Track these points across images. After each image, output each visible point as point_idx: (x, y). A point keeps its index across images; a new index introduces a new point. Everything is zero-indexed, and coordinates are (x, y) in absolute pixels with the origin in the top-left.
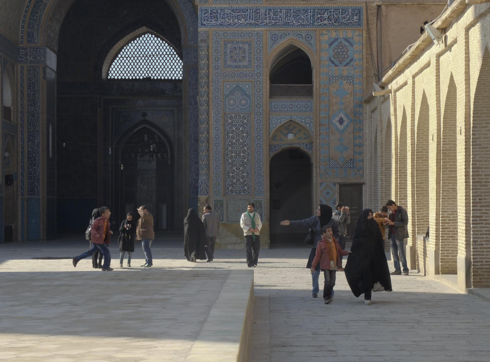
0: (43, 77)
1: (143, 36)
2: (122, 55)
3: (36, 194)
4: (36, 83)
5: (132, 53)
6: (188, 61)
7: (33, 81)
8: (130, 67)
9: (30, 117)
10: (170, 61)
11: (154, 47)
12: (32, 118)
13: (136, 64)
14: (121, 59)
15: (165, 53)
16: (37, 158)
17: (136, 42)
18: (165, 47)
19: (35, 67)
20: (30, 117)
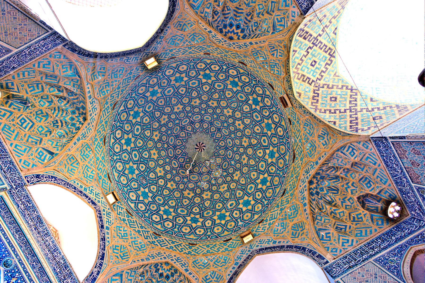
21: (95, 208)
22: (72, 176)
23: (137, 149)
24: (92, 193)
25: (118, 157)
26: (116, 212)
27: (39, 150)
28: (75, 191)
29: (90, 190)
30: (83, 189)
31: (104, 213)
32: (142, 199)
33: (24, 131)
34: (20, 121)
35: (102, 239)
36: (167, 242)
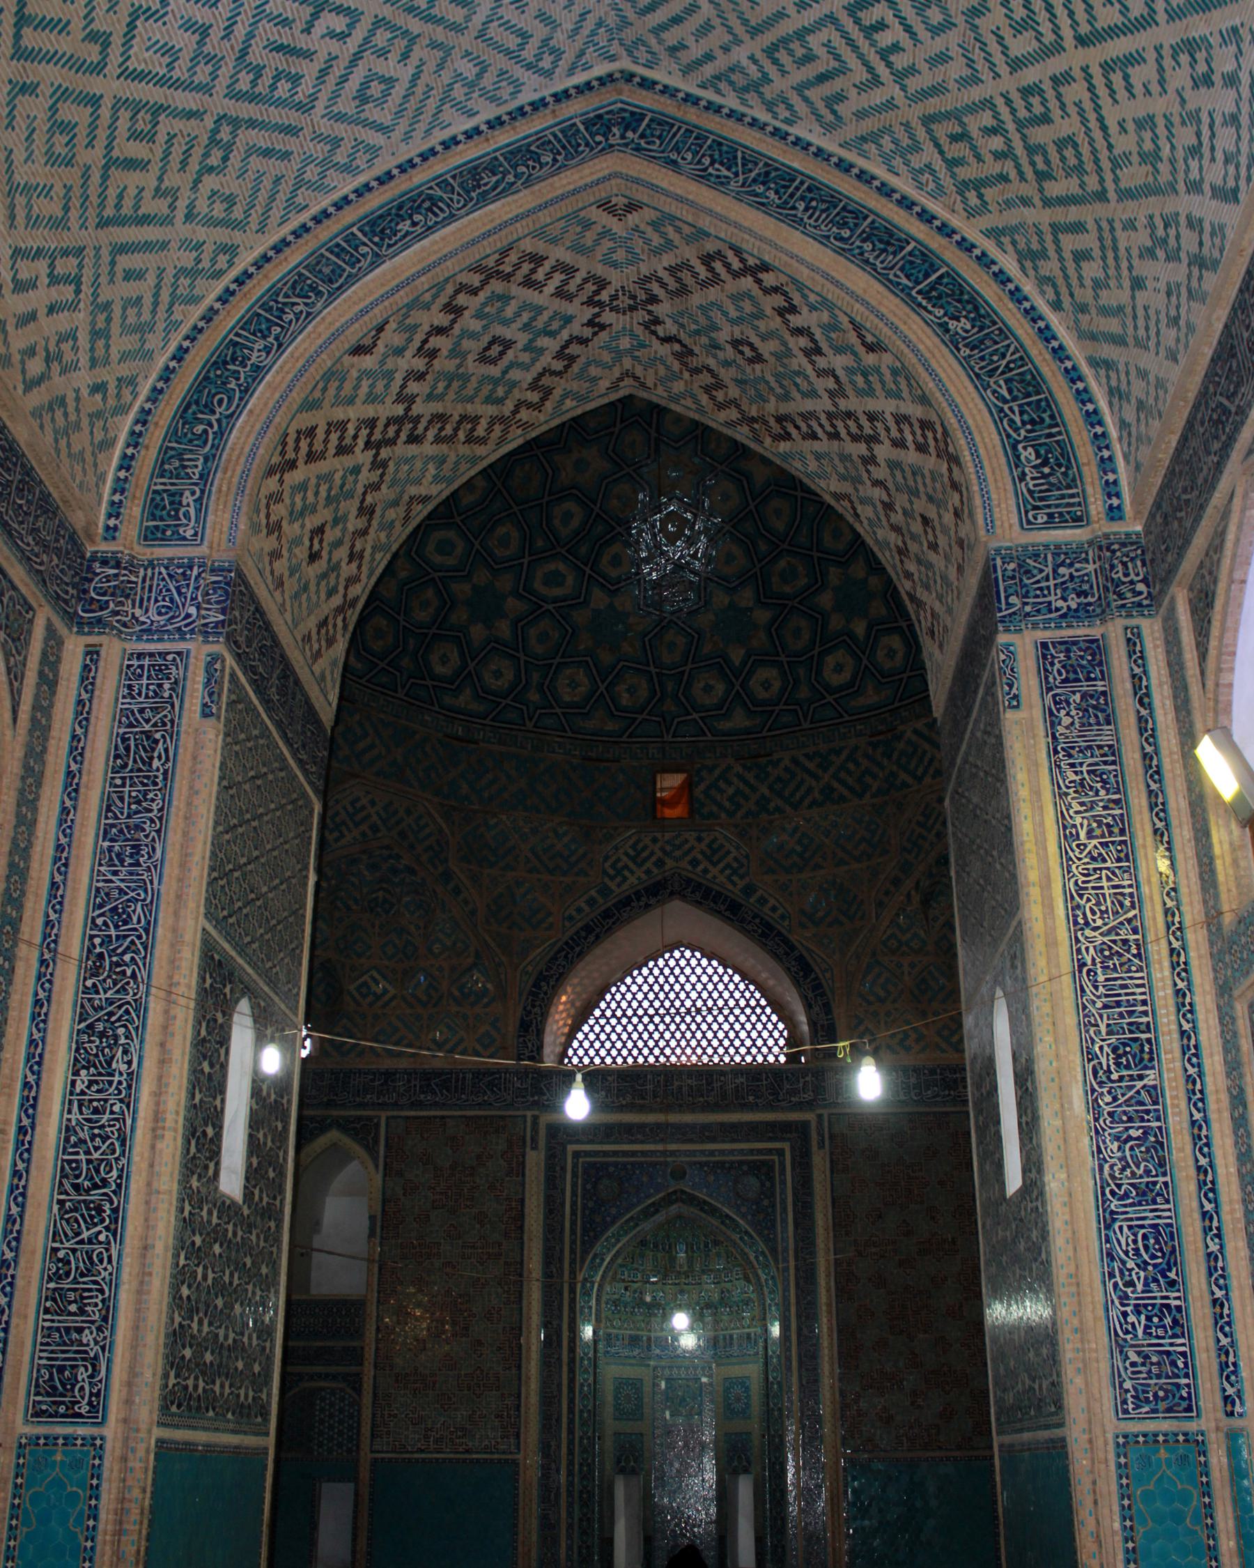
0: (205, 705)
1: (667, 956)
2: (603, 1011)
3: (84, 1409)
4: (158, 736)
5: (635, 1004)
6: (1028, 609)
7: (147, 727)
8: (630, 1044)
9: (99, 921)
10: (748, 1026)
11: (699, 987)
12: (113, 933)
13: (646, 1036)
14: (603, 1022)
15: (732, 1003)
16: (115, 1173)
17: (645, 971)
18: (732, 987)
19: (163, 655)
20: (99, 921)
21: (672, 893)
22: (551, 919)
23: (526, 561)
24: (626, 873)
25: (536, 677)
26: (723, 815)
27: (457, 993)
28: (597, 937)
29: (612, 872)
30: (601, 901)
31: (701, 867)
32: (742, 652)
33: (394, 997)
34: (364, 996)
35: (764, 935)
36: (927, 746)
